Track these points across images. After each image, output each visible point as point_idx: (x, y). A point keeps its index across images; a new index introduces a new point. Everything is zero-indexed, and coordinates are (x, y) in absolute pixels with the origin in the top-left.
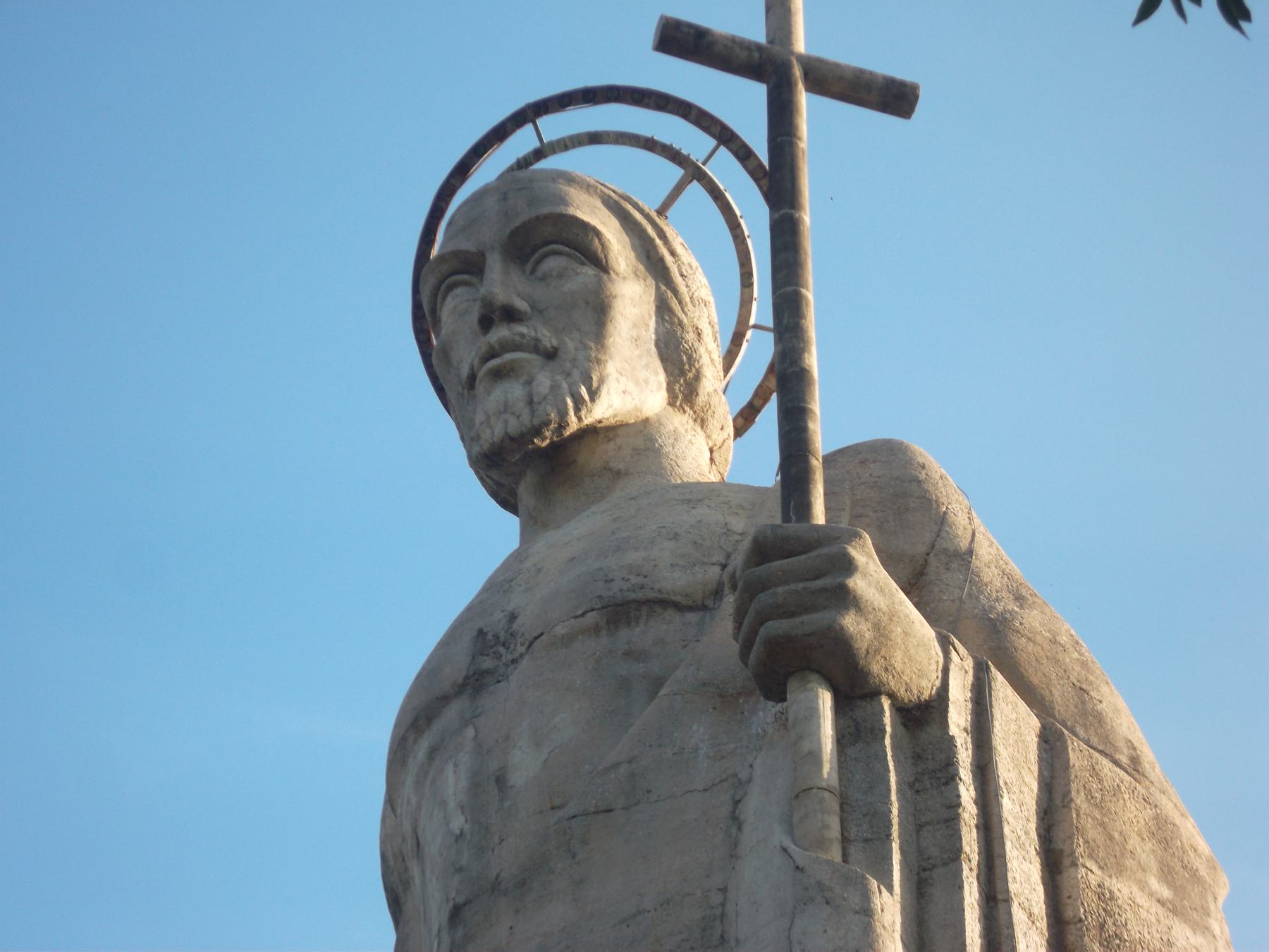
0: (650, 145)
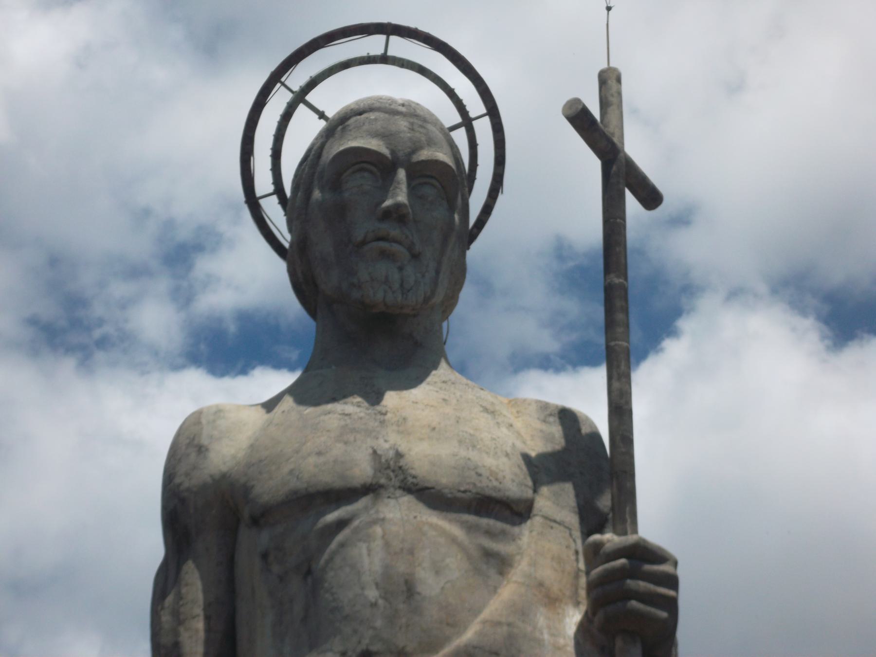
0: (450, 93)
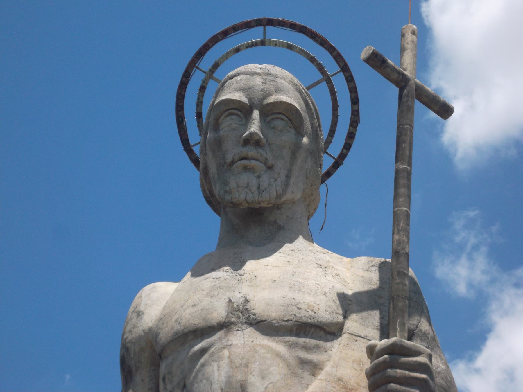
0: (312, 60)
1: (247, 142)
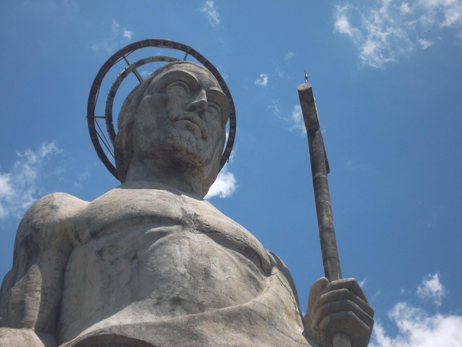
1: (193, 108)
